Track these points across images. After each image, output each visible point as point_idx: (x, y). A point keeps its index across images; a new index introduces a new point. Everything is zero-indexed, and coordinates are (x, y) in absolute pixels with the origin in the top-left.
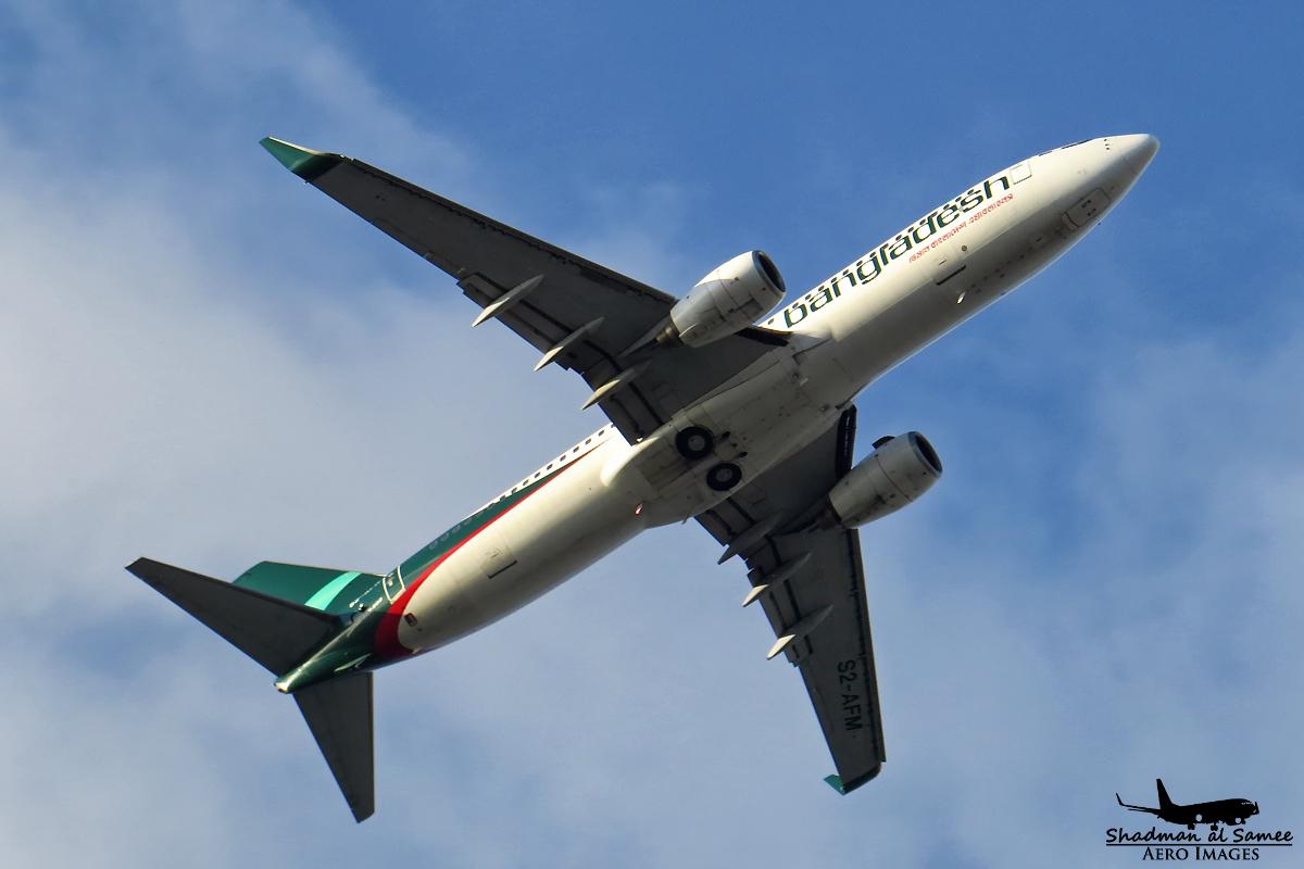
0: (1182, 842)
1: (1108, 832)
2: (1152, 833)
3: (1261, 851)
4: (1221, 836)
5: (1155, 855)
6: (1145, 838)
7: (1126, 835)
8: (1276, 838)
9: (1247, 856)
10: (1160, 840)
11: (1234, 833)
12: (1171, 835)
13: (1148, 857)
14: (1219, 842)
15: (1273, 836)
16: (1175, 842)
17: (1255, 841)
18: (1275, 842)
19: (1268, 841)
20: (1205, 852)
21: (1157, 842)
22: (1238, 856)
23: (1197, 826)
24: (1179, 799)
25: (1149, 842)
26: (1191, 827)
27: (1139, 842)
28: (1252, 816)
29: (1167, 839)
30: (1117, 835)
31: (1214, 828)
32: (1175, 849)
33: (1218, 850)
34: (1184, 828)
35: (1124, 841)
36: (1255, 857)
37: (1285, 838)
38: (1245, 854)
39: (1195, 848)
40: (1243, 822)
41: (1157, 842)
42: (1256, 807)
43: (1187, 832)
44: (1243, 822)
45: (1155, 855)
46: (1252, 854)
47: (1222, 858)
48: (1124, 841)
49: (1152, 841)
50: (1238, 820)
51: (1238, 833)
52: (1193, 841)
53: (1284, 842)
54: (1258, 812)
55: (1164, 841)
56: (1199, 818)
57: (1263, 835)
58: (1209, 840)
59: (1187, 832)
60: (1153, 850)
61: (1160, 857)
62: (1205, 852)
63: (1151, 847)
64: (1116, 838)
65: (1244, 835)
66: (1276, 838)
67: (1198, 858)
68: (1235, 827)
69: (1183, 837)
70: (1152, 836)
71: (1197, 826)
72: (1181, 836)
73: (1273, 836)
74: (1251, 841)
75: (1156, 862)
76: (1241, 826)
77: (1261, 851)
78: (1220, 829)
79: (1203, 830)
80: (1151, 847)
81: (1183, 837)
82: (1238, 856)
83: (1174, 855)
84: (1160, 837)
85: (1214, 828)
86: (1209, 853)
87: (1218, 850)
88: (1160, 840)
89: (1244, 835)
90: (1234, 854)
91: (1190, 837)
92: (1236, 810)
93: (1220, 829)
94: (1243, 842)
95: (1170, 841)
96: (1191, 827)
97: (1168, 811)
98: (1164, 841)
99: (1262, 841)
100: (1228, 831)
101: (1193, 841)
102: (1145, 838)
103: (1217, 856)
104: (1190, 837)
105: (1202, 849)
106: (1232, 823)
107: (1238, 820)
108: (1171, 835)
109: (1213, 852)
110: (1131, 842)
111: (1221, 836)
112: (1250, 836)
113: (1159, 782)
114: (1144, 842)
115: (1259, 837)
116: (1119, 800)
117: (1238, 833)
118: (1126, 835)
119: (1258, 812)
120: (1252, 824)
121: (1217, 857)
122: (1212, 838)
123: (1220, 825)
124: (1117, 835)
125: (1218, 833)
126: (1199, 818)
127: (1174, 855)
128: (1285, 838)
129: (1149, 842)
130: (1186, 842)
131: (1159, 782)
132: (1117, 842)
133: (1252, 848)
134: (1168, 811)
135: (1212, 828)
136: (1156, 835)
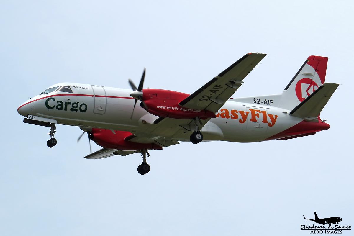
0: (321, 229)
1: (301, 226)
2: (313, 226)
3: (343, 231)
4: (332, 227)
5: (314, 232)
6: (311, 228)
7: (306, 227)
8: (347, 228)
9: (339, 233)
10: (317, 228)
11: (335, 226)
12: (318, 227)
13: (312, 233)
14: (331, 229)
15: (346, 227)
16: (319, 229)
17: (341, 228)
18: (346, 229)
19: (345, 228)
20: (328, 231)
21: (314, 229)
22: (336, 232)
23: (325, 224)
24: (320, 217)
25: (312, 229)
26: (324, 225)
27: (309, 229)
28: (340, 222)
29: (317, 228)
30: (304, 227)
31: (330, 225)
32: (319, 230)
33: (331, 231)
34: (322, 225)
35: (306, 228)
36: (341, 233)
37: (349, 228)
38: (338, 232)
39: (325, 230)
40: (338, 223)
41: (314, 229)
42: (341, 219)
43: (323, 226)
44: (338, 223)
45: (314, 232)
46: (340, 231)
47: (332, 233)
48: (306, 228)
49: (313, 228)
50: (336, 223)
51: (336, 226)
52: (324, 228)
53: (349, 229)
54: (342, 221)
55: (316, 228)
56: (326, 222)
57: (343, 227)
58: (329, 228)
59: (323, 226)
60: (313, 231)
61: (315, 233)
62: (328, 231)
63: (313, 230)
64: (303, 227)
65: (338, 227)
66: (347, 228)
67: (325, 233)
68: (335, 225)
69: (321, 227)
70: (313, 227)
71: (325, 224)
72: (321, 227)
73: (346, 227)
74: (340, 229)
75: (314, 234)
76: (337, 224)
77: (343, 231)
78: (331, 225)
79: (327, 225)
80: (313, 230)
81: (321, 227)
82: (336, 232)
83: (319, 232)
84: (315, 227)
85: (330, 225)
86: (329, 232)
87: (331, 231)
88: (315, 228)
89: (338, 227)
90: (335, 232)
91: (323, 227)
92: (336, 220)
93: (331, 225)
94: (338, 229)
95: (318, 228)
96: (324, 225)
97: (317, 220)
98: (316, 228)
99: (343, 228)
100: (334, 226)
101: (324, 228)
102: (311, 228)
103: (331, 232)
104: (323, 227)
105: (327, 231)
106: (335, 223)
107: (336, 223)
108: (318, 227)
109: (330, 231)
110: (307, 229)
111: (332, 227)
112: (340, 227)
113: (315, 212)
114: (311, 229)
115: (342, 228)
116: (305, 218)
117: (336, 226)
118: (306, 227)
119: (342, 221)
120: (340, 224)
121: (331, 233)
122: (329, 227)
123: (332, 224)
124: (304, 227)
125: (331, 226)
126: (326, 222)
127: (319, 232)
128: (349, 228)
129: (312, 229)
130: (322, 229)
131: (315, 212)
132: (303, 229)
133: (340, 230)
134: (317, 220)
135: (329, 225)
136: (314, 227)
